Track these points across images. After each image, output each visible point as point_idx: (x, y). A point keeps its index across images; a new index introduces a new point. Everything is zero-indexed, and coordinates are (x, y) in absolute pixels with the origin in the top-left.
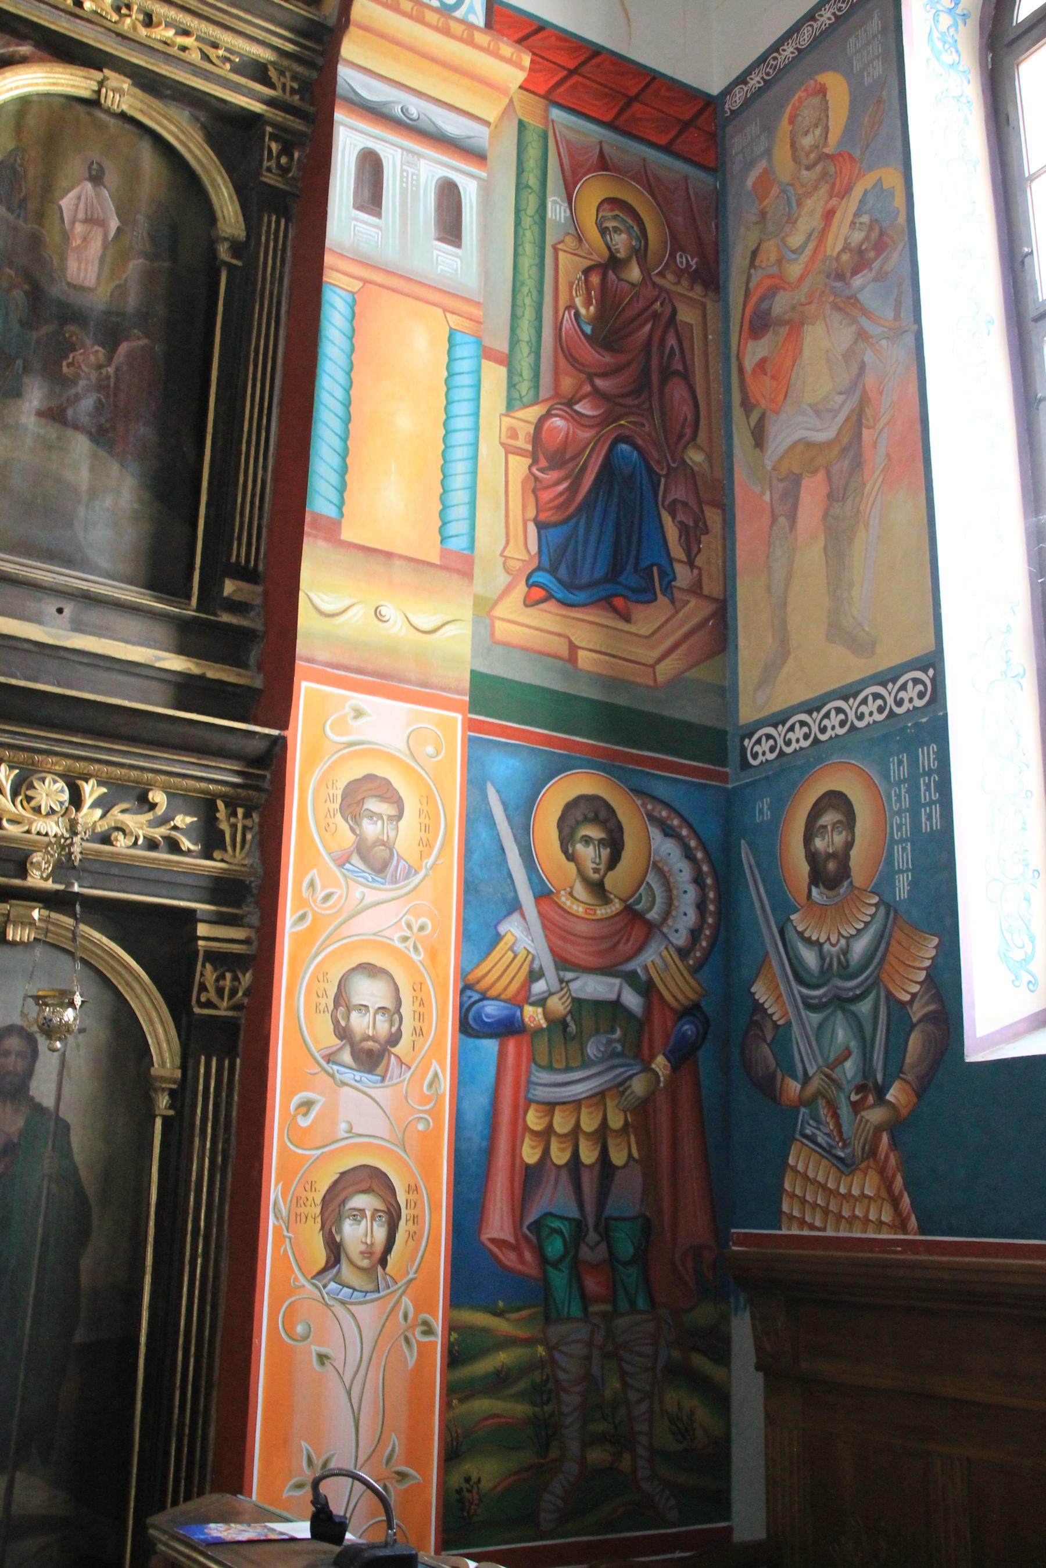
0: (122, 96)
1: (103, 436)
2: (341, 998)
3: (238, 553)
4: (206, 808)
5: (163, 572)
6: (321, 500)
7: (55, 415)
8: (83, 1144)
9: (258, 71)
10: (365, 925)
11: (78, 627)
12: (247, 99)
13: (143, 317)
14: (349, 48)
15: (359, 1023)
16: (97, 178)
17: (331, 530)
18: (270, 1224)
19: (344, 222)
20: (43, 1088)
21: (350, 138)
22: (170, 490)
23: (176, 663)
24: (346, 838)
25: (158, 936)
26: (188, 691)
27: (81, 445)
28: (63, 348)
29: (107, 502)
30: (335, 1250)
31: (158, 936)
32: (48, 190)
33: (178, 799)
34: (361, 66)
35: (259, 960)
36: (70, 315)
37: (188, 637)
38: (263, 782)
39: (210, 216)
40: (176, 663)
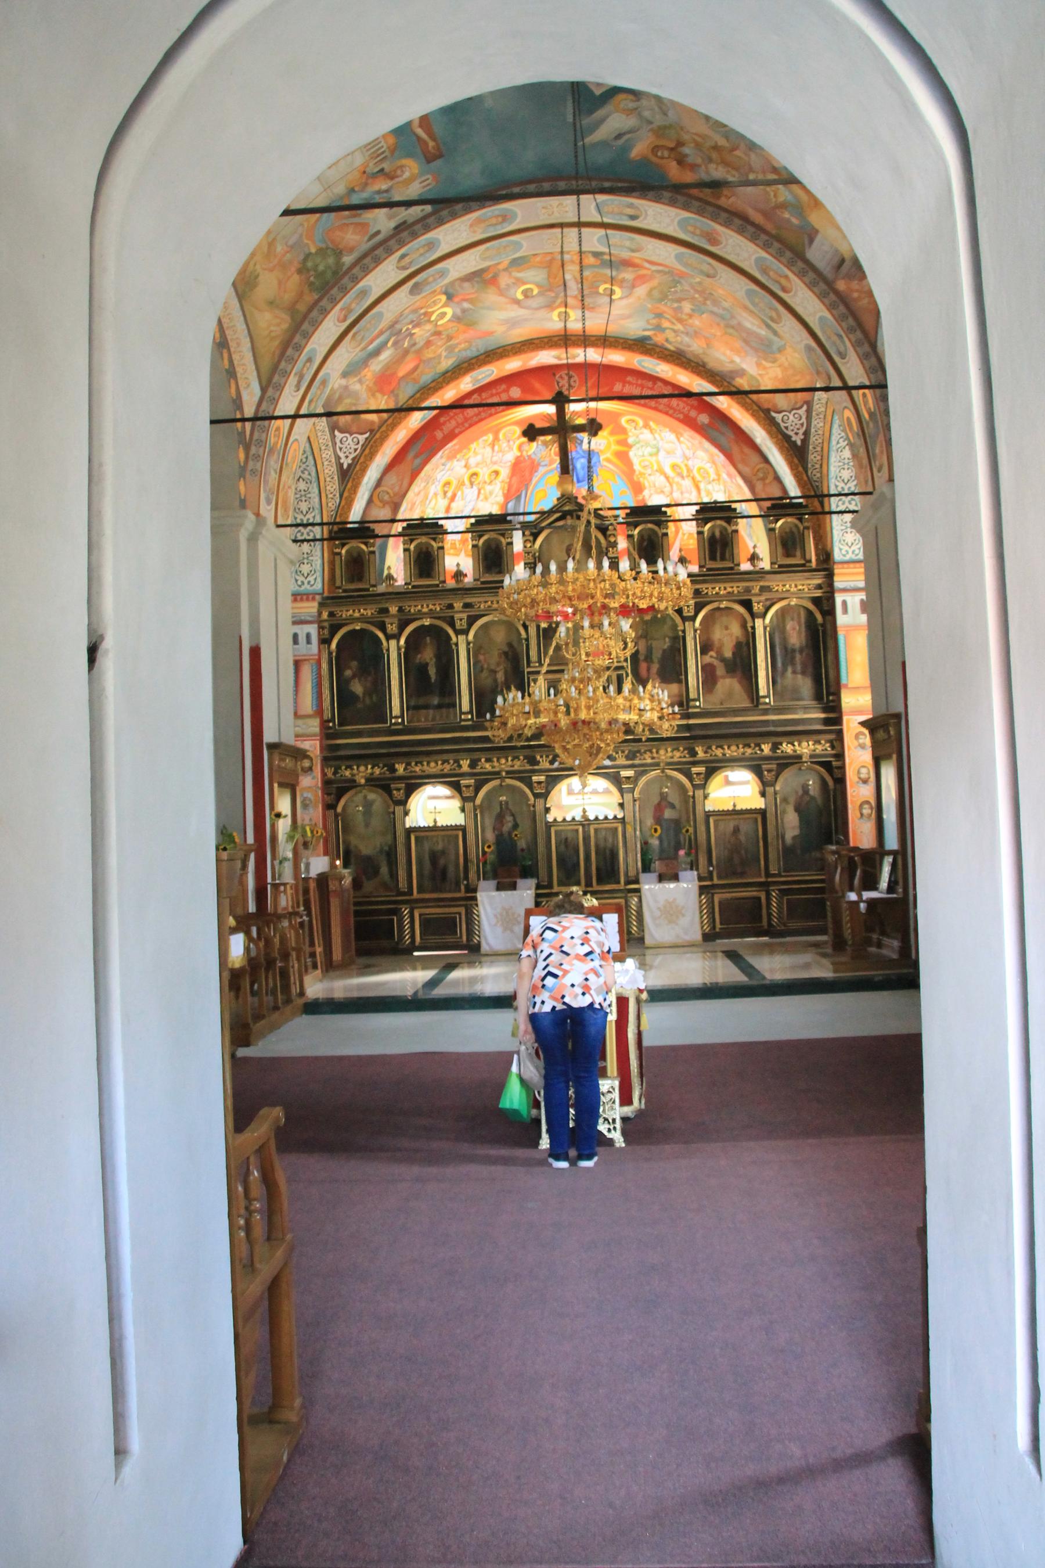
0: (794, 602)
1: (803, 673)
2: (859, 772)
3: (832, 690)
4: (831, 742)
5: (818, 697)
6: (843, 681)
7: (794, 672)
8: (820, 801)
9: (819, 587)
10: (862, 758)
11: (805, 713)
12: (818, 593)
13: (807, 646)
14: (836, 578)
15: (862, 776)
16: (793, 619)
17: (846, 686)
18: (850, 812)
19: (841, 619)
20: (811, 793)
21: (839, 599)
22: (817, 680)
23: (823, 716)
24: (856, 743)
25: (827, 765)
26: (827, 722)
27: (799, 676)
28: (793, 658)
29: (805, 685)
30: (862, 815)
31: (827, 765)
32: (784, 627)
33: (827, 741)
34: (839, 583)
35: (842, 768)
36: (793, 651)
37: (825, 710)
38: (840, 733)
39: (815, 619)
40: (823, 716)
